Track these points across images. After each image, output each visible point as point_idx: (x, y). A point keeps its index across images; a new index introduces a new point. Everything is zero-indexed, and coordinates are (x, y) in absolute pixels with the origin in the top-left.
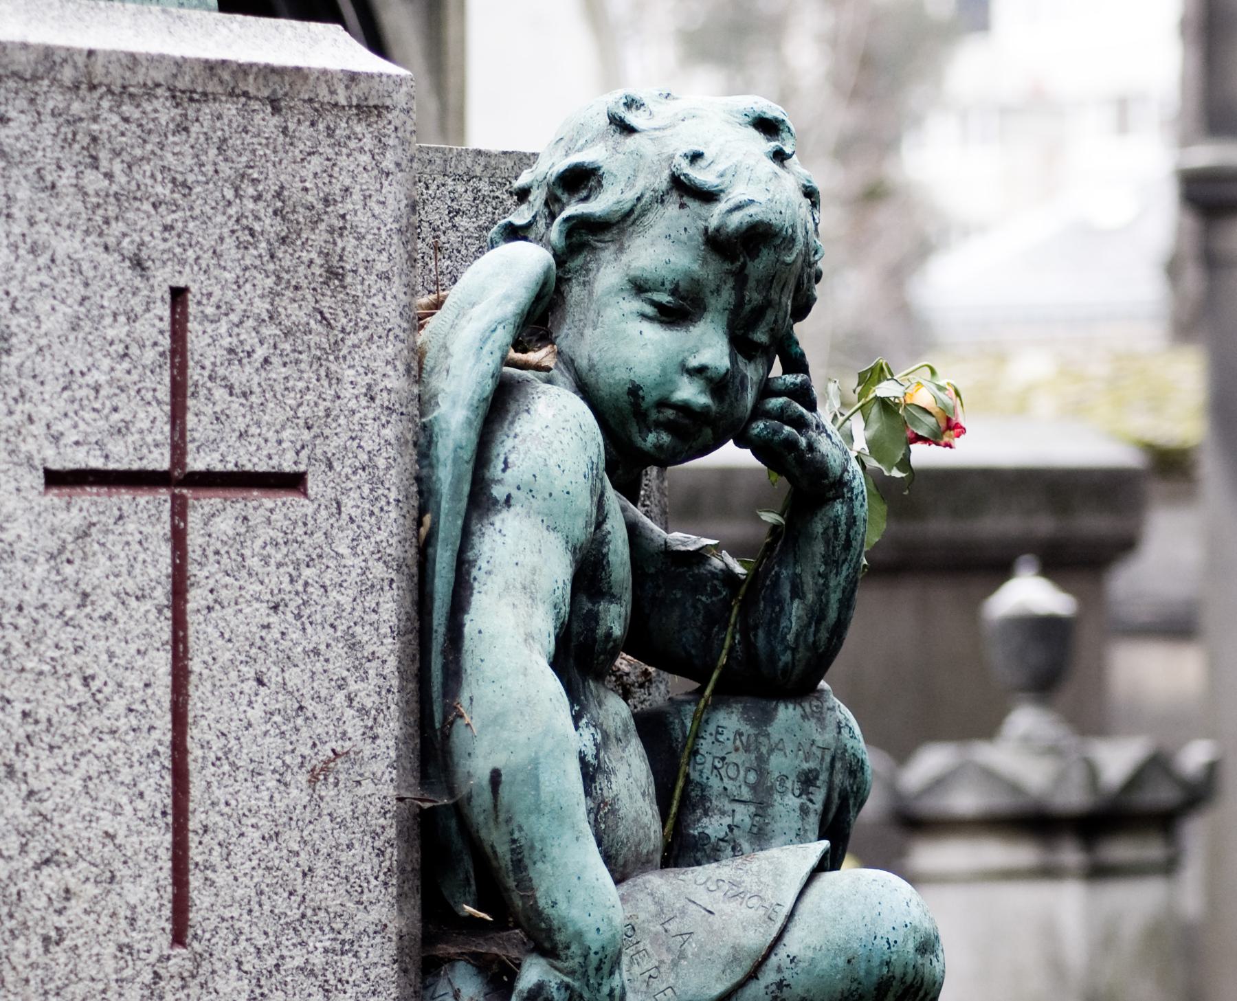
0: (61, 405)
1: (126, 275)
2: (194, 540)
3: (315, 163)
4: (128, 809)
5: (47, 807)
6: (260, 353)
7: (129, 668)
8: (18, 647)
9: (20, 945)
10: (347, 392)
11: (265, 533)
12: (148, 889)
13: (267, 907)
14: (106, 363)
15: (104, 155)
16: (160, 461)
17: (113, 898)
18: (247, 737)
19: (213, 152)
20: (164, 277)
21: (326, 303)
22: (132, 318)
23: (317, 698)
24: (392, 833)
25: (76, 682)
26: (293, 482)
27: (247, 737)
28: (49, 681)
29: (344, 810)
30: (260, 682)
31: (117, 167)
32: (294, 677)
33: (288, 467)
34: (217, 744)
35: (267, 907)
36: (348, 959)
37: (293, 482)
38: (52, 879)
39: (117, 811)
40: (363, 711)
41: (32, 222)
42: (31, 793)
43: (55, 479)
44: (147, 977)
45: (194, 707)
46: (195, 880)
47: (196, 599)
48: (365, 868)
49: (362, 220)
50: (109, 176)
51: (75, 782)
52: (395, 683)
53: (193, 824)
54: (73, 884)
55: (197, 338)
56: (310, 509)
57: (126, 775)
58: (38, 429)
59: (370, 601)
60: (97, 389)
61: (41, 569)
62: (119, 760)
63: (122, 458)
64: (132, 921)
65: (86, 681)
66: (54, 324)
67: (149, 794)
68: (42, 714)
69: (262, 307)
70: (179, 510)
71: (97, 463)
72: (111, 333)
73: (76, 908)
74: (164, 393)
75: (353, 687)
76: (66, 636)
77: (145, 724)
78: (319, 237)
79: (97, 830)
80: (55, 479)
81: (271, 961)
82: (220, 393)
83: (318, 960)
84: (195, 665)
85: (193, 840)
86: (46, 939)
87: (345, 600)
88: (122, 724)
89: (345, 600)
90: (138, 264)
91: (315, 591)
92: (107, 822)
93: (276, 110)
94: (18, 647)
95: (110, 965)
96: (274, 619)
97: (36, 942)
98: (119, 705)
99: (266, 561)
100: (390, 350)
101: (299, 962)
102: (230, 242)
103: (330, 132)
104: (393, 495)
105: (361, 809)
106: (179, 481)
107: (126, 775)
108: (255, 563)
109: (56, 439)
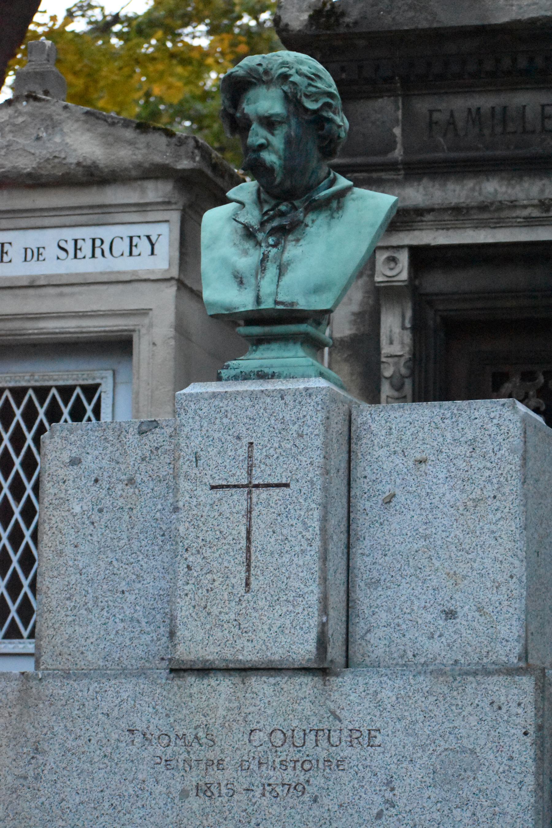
0: (215, 471)
1: (235, 441)
2: (254, 500)
3: (295, 410)
4: (232, 562)
5: (209, 561)
6: (275, 456)
7: (234, 529)
8: (201, 525)
9: (200, 591)
10: (304, 463)
11: (276, 498)
12: (238, 580)
13: (275, 585)
14: (228, 461)
15: (229, 415)
16: (245, 482)
17: (227, 582)
18: (269, 545)
19: (262, 411)
20: (245, 441)
21: (297, 443)
22: (236, 450)
23: (292, 536)
24: (317, 569)
25: (218, 533)
26: (287, 485)
27: (269, 545)
28: (210, 532)
29: (301, 563)
30: (274, 533)
31: (233, 417)
32: (285, 531)
33: (284, 481)
34: (260, 547)
35: (275, 585)
36: (301, 599)
37: (287, 485)
38: (209, 576)
39: (229, 562)
40: (308, 540)
41: (207, 431)
42: (204, 558)
43: (213, 487)
44: (237, 600)
45: (253, 538)
46: (252, 579)
47: (254, 514)
48: (308, 577)
49: (309, 422)
50: (231, 419)
51: (217, 555)
52: (318, 532)
53: (253, 565)
54: (215, 578)
55: (256, 454)
56: (291, 492)
57: (232, 554)
58: (208, 476)
59: (310, 513)
60: (225, 467)
61: (208, 507)
62: (231, 550)
63: (232, 481)
64: (233, 587)
65: (221, 532)
66: (213, 452)
67: (239, 558)
68: (208, 540)
69: (276, 445)
70: (250, 493)
71: (225, 483)
72: (230, 454)
73: (216, 584)
74: (245, 466)
75: (304, 534)
76: (215, 523)
77: (238, 542)
78: (296, 427)
79: (223, 566)
80: (213, 487)
81: (276, 598)
82: (263, 467)
83: (291, 599)
84: (254, 528)
85: (252, 569)
86: (208, 590)
87: (302, 513)
88: (231, 542)
89: (302, 513)
90: (238, 438)
91: (292, 511)
92: (226, 564)
93: (282, 398)
94: (201, 525)
95: (226, 597)
96: (278, 518)
97: (205, 590)
98: (230, 538)
99: (276, 504)
100: (318, 452)
101: (285, 598)
102: (267, 431)
103: (300, 403)
104: (318, 487)
105: (306, 563)
106: (251, 487)
107: (232, 554)
108: (273, 505)
109: (213, 478)
